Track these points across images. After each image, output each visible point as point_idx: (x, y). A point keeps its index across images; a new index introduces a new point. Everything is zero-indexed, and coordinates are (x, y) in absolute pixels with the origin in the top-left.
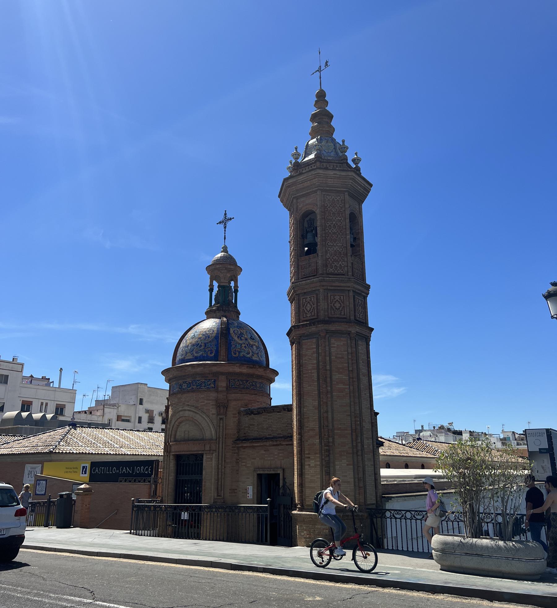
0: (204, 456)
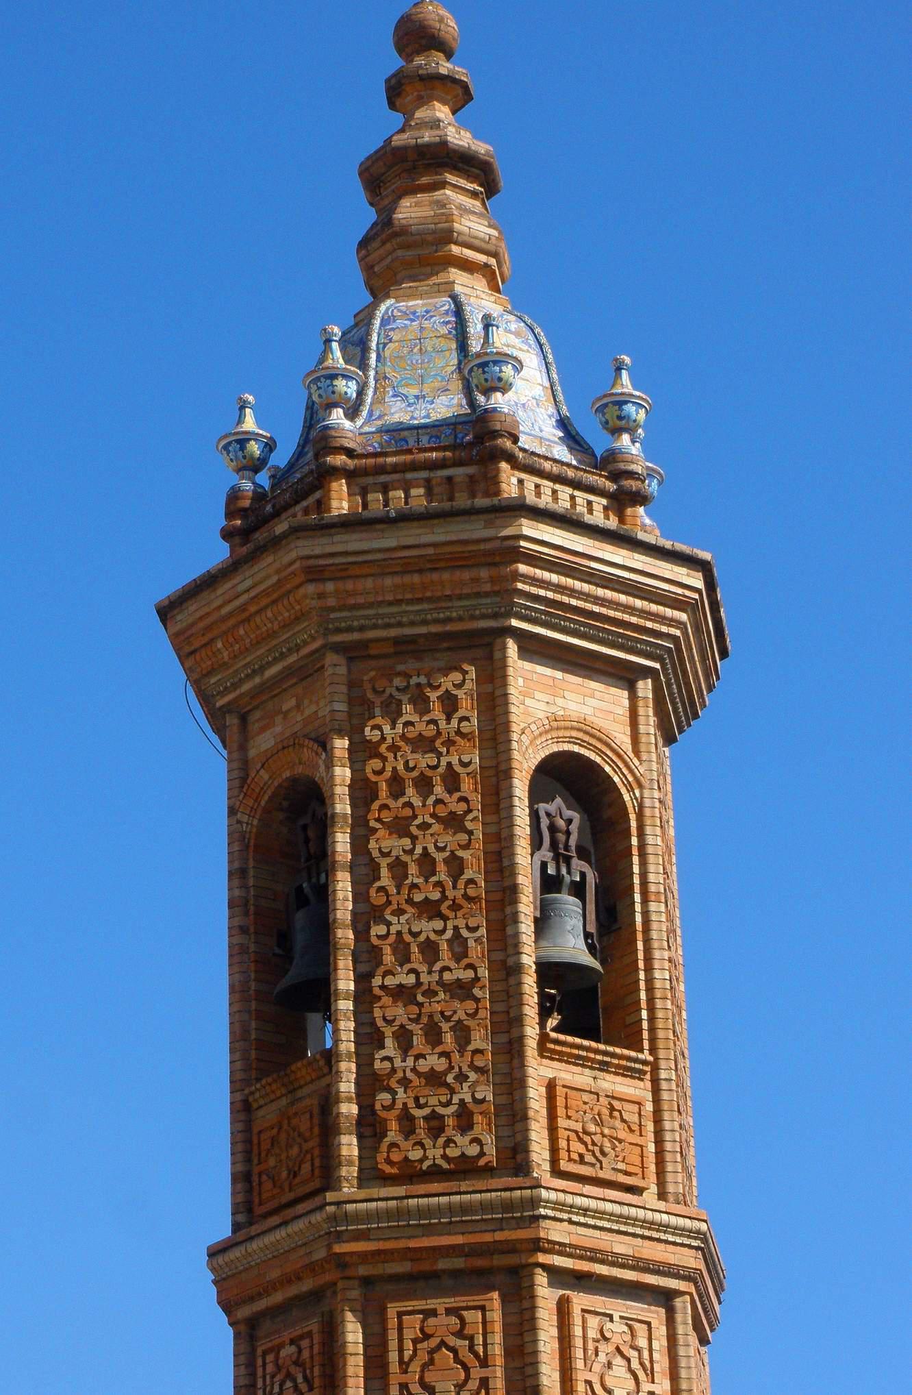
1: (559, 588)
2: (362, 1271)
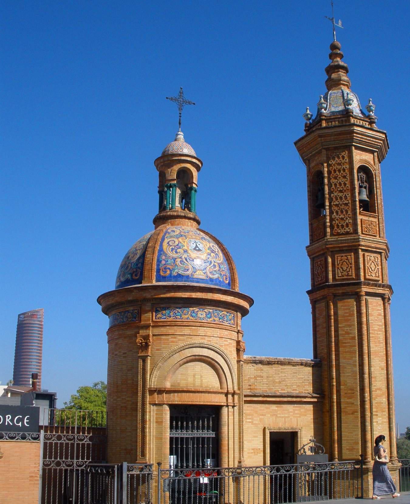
0: (225, 410)
1: (361, 138)
2: (331, 250)
